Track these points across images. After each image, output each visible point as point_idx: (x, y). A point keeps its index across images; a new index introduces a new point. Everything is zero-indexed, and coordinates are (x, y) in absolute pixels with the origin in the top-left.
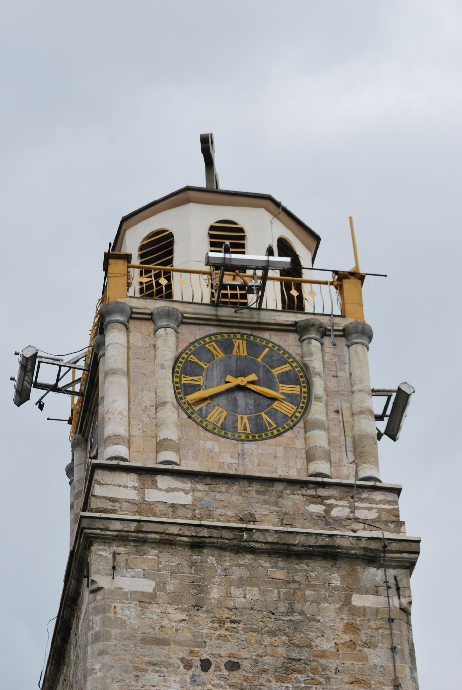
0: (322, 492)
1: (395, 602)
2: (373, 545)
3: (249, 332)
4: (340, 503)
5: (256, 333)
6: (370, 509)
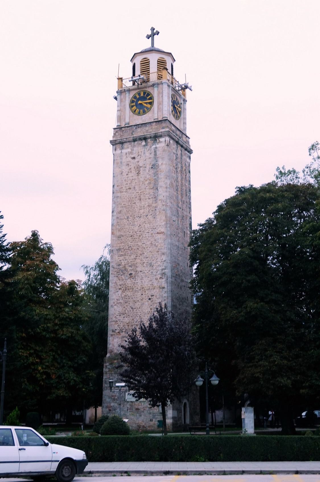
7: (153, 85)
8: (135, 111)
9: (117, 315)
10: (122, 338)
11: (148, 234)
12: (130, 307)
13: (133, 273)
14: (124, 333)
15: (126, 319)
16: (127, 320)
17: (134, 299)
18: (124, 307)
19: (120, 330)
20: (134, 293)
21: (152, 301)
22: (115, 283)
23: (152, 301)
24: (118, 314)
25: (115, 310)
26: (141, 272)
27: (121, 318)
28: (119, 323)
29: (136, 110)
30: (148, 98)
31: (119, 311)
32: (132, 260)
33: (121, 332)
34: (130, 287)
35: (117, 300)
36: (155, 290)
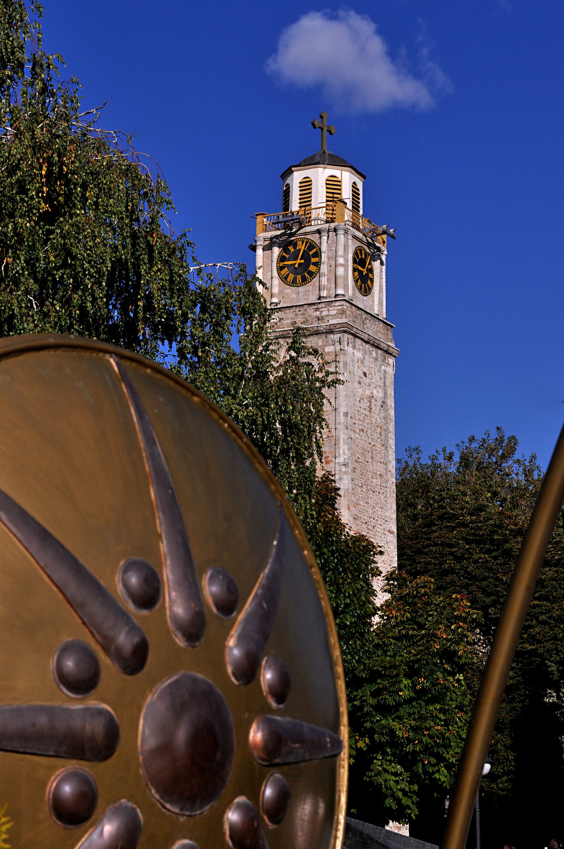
0: (320, 306)
1: (338, 348)
2: (332, 327)
3: (303, 237)
4: (325, 309)
5: (305, 237)
6: (334, 310)
7: (319, 232)
8: (286, 278)
29: (288, 274)
30: (311, 253)
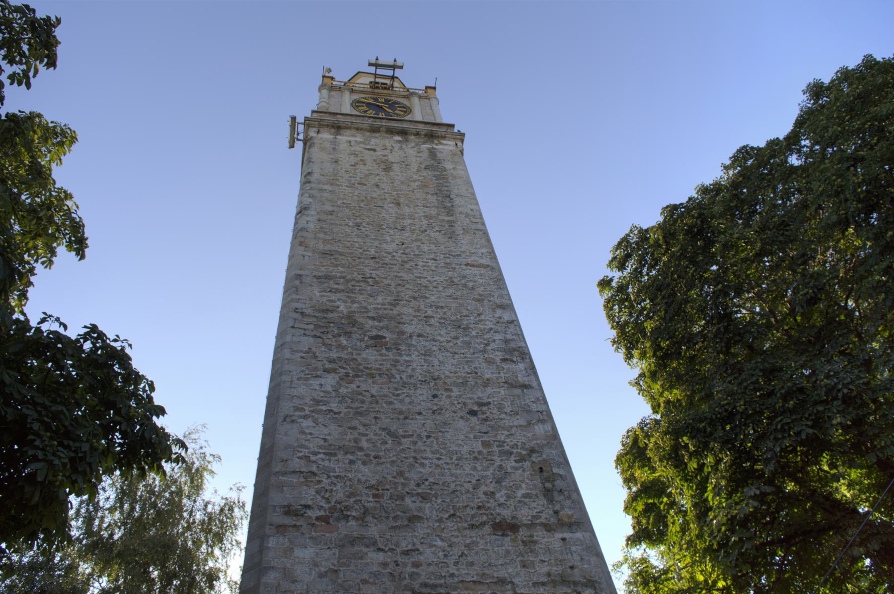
9: (315, 454)
10: (343, 546)
11: (432, 261)
12: (384, 429)
13: (387, 335)
14: (352, 523)
15: (365, 469)
16: (367, 473)
17: (398, 405)
18: (354, 428)
19: (332, 510)
20: (397, 389)
21: (486, 420)
22: (307, 352)
23: (486, 420)
24: (320, 447)
25: (303, 433)
26: (419, 336)
27: (337, 466)
28: (325, 481)
31: (325, 440)
32: (380, 306)
33: (338, 519)
34: (379, 369)
35: (317, 402)
36: (489, 390)
